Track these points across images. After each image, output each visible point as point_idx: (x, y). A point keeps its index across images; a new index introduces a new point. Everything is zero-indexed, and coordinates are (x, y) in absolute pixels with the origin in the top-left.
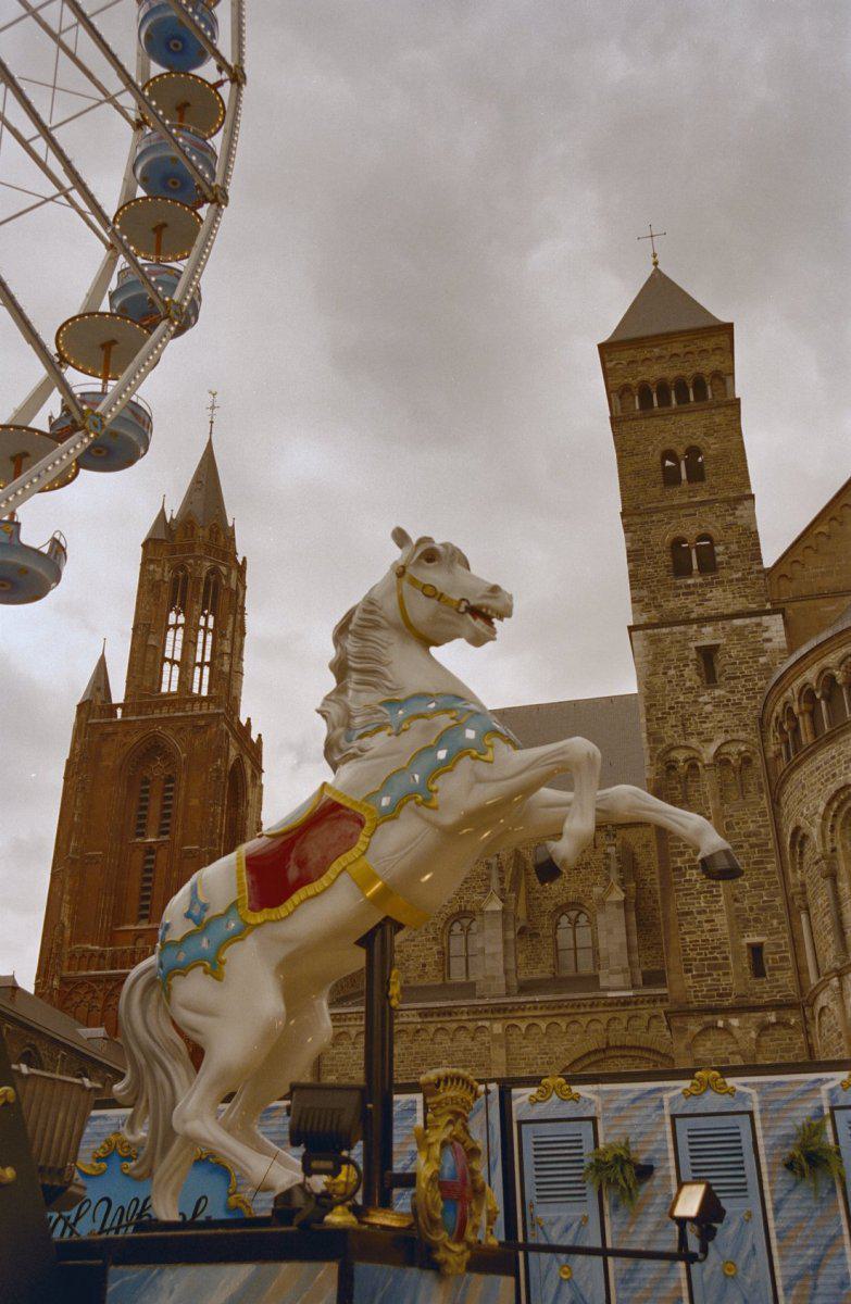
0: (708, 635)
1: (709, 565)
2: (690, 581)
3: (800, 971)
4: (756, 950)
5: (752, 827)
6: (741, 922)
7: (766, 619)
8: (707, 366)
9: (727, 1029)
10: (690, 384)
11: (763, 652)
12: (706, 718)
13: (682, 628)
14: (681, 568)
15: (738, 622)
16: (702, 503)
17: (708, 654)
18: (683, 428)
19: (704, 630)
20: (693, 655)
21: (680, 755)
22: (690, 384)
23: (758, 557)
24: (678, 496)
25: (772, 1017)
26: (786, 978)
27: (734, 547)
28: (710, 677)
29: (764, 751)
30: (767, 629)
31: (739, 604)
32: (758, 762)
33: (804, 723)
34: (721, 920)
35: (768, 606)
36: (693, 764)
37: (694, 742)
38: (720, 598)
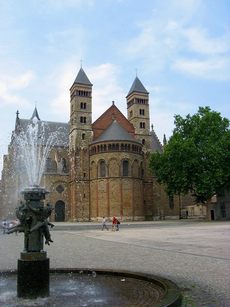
1: (85, 122)
3: (90, 177)
4: (85, 173)
5: (86, 159)
6: (83, 170)
7: (91, 131)
8: (89, 90)
9: (81, 183)
10: (86, 93)
11: (90, 136)
13: (81, 130)
14: (81, 121)
15: (88, 131)
16: (85, 112)
17: (83, 134)
18: (84, 100)
22: (86, 93)
23: (91, 122)
24: (83, 110)
25: (86, 182)
26: (88, 177)
28: (83, 138)
29: (89, 149)
30: (91, 133)
32: (88, 150)
33: (97, 149)
34: (81, 170)
35: (91, 130)
36: (80, 149)
37: (80, 146)
38: (87, 127)
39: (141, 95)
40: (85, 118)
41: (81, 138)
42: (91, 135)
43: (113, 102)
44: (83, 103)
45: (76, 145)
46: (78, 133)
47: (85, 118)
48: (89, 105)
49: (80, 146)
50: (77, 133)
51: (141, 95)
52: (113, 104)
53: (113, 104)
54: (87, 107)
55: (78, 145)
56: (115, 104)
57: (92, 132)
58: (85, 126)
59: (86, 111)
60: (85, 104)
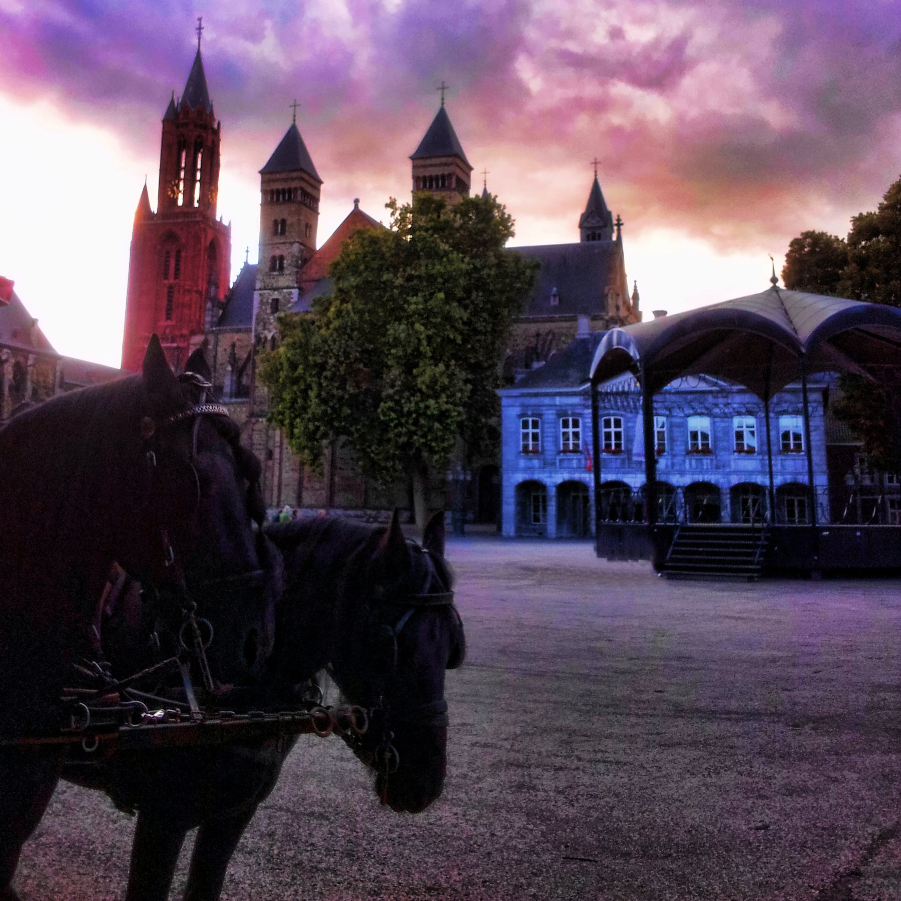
0: (276, 295)
1: (282, 268)
2: (275, 273)
7: (293, 291)
11: (289, 302)
12: (271, 324)
14: (273, 268)
15: (285, 291)
17: (276, 301)
19: (276, 293)
20: (270, 301)
21: (262, 336)
27: (290, 262)
31: (287, 284)
36: (266, 338)
38: (283, 281)
39: (431, 165)
40: (282, 258)
41: (269, 311)
42: (292, 300)
43: (357, 201)
44: (279, 220)
45: (256, 330)
46: (261, 301)
47: (282, 258)
48: (292, 225)
49: (266, 332)
50: (259, 299)
51: (431, 165)
52: (356, 206)
53: (356, 206)
54: (287, 229)
55: (260, 328)
56: (363, 207)
57: (295, 292)
58: (281, 279)
59: (285, 241)
60: (284, 222)
